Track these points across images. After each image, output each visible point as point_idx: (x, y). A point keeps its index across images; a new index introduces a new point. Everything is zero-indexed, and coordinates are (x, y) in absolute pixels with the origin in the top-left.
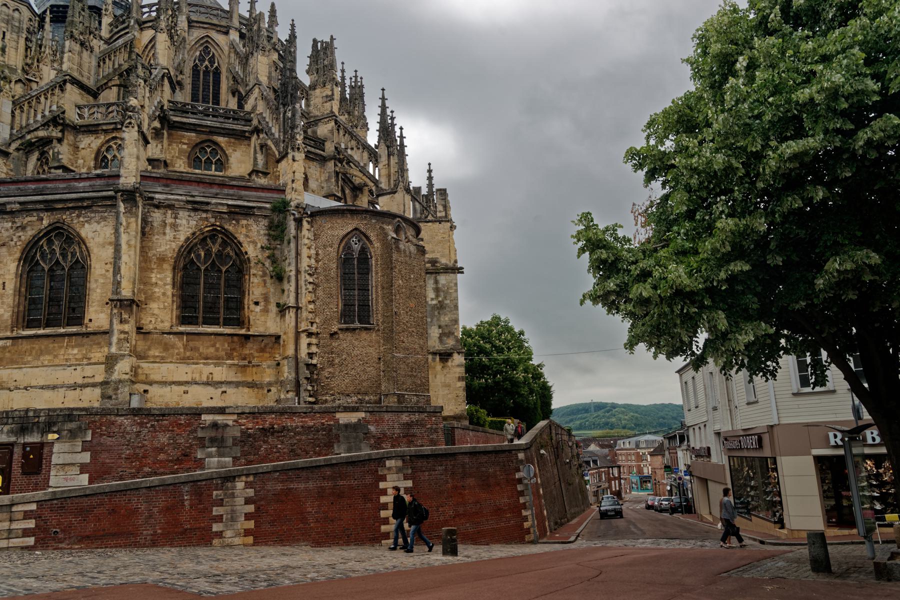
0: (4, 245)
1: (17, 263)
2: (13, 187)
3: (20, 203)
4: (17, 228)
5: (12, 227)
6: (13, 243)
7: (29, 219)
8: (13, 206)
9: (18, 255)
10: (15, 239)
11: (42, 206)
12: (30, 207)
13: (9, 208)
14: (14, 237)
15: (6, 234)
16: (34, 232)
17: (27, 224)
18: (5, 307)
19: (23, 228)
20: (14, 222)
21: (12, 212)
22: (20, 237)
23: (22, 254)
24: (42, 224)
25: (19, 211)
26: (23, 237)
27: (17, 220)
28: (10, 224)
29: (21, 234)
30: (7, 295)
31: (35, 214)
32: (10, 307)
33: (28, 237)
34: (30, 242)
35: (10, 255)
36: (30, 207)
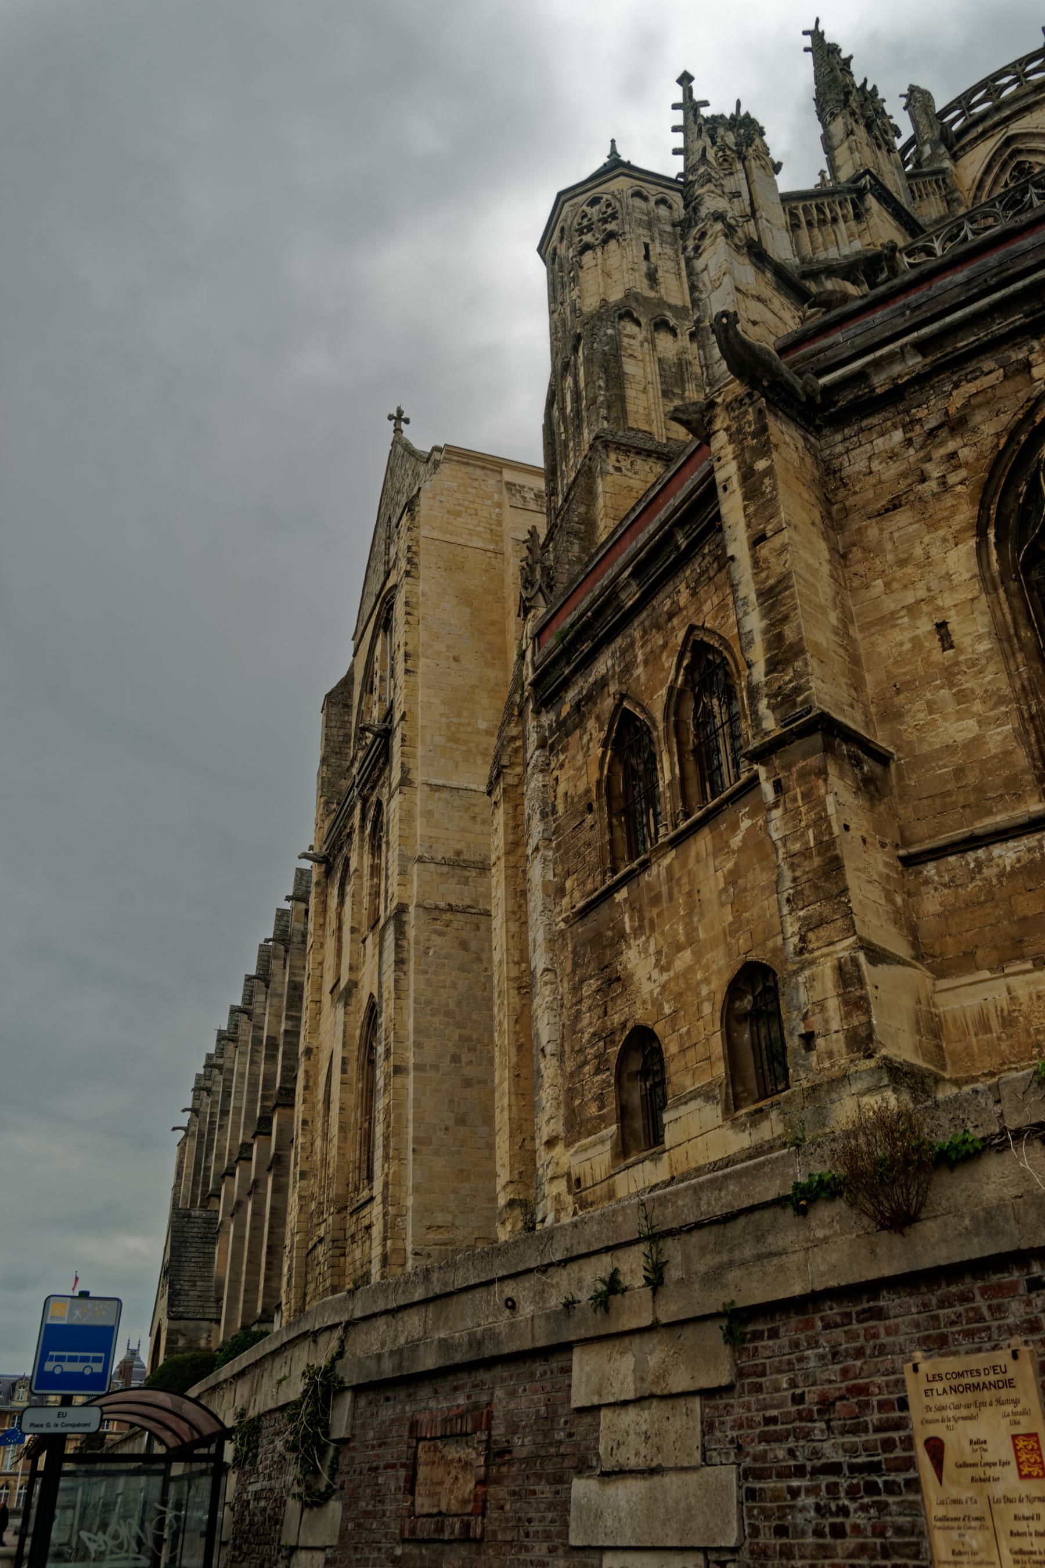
0: (895, 507)
1: (973, 542)
2: (879, 315)
3: (922, 347)
4: (932, 433)
5: (909, 442)
6: (932, 485)
7: (971, 388)
8: (897, 369)
9: (967, 513)
10: (934, 471)
11: (1017, 319)
12: (965, 342)
13: (880, 382)
14: (928, 467)
15: (889, 471)
16: (1005, 418)
17: (964, 406)
18: (977, 707)
19: (956, 424)
20: (907, 427)
21: (897, 395)
22: (953, 455)
23: (984, 506)
24: (1032, 380)
25: (921, 380)
26: (966, 454)
27: (921, 413)
28: (898, 436)
29: (951, 446)
30: (973, 663)
31: (988, 365)
32: (1002, 700)
33: (989, 442)
34: (1001, 454)
35: (933, 526)
36: (965, 342)
